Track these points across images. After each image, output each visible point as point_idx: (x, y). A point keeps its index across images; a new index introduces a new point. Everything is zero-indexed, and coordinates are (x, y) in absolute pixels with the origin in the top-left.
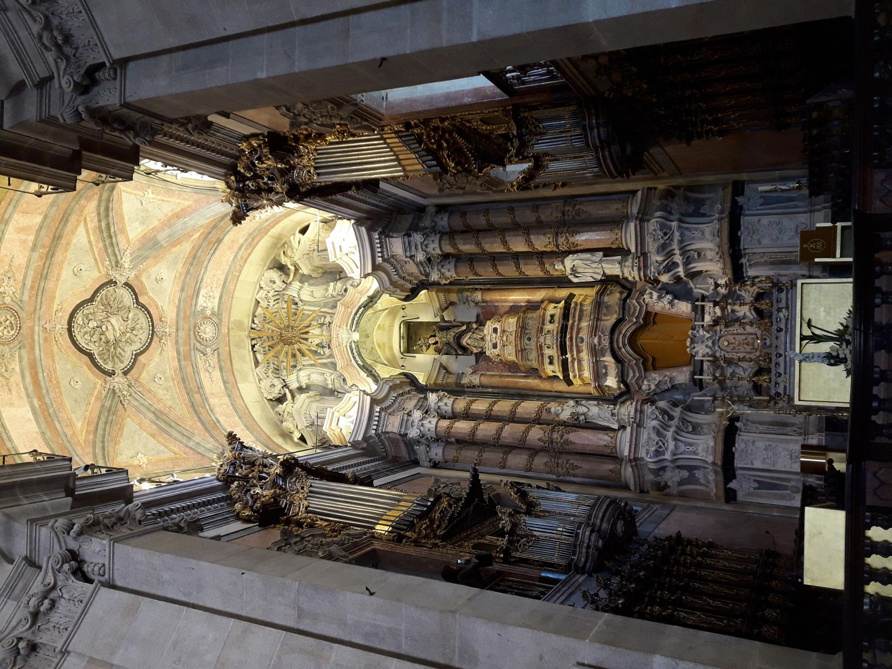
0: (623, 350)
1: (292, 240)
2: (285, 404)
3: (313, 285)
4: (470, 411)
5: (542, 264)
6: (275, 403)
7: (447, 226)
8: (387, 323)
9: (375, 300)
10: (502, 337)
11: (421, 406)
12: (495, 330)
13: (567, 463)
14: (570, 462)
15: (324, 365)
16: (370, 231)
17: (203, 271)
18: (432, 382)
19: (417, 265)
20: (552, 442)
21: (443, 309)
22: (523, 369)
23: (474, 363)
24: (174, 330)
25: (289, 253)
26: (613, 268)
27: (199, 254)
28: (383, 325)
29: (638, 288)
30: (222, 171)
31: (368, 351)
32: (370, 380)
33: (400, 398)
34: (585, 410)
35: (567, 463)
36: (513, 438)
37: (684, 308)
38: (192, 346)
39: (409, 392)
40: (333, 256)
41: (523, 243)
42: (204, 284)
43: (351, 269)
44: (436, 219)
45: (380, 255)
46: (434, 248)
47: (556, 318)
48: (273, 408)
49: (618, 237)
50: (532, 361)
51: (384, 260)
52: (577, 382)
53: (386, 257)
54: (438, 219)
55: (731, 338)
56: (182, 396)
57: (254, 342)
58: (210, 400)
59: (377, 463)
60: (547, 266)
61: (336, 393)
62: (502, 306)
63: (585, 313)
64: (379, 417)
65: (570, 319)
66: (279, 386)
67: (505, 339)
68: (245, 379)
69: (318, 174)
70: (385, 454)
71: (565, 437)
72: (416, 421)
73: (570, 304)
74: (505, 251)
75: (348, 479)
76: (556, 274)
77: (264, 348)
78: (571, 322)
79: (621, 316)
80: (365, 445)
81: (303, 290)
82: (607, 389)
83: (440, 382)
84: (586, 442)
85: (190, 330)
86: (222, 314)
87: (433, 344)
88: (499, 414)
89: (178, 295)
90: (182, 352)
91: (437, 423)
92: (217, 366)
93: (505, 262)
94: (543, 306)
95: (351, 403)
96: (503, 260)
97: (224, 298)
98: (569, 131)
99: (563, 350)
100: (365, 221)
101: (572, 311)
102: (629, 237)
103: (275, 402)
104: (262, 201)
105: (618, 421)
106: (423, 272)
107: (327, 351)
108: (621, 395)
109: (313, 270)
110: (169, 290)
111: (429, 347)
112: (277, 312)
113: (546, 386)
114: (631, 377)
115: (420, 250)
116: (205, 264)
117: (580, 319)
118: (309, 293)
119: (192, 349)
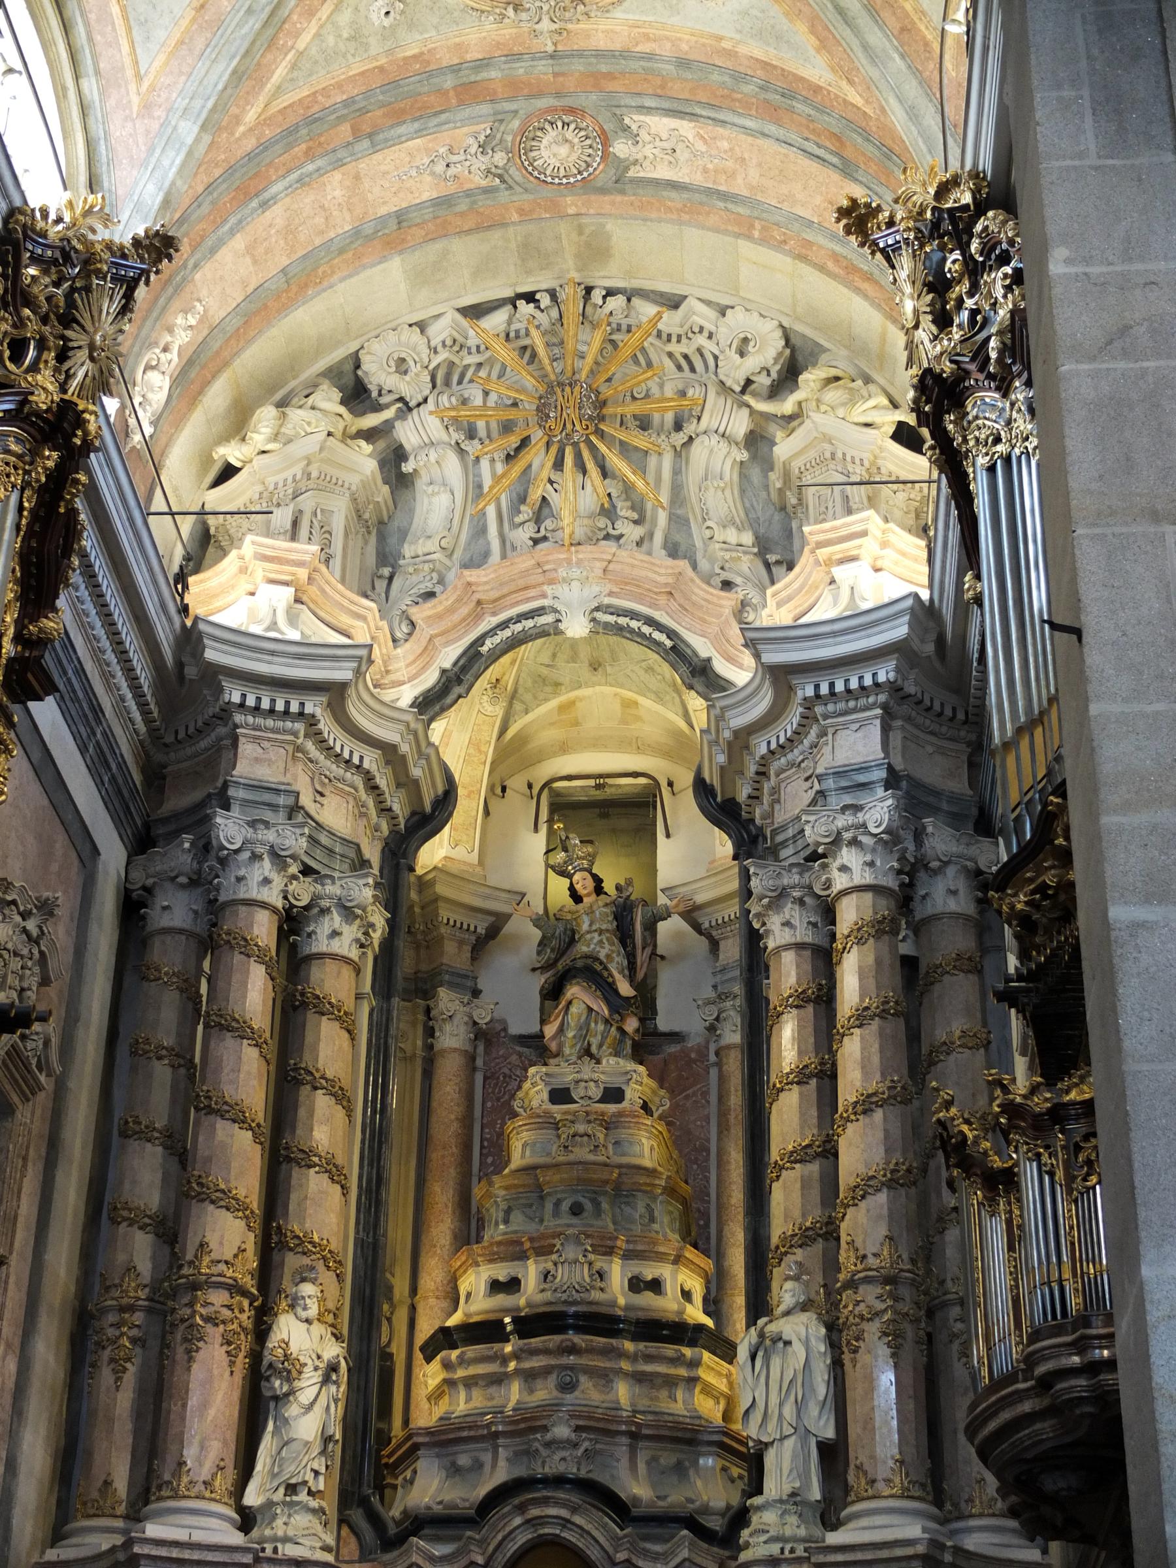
0: (518, 1521)
1: (872, 403)
2: (342, 410)
3: (743, 476)
4: (311, 1016)
5: (805, 1237)
6: (349, 380)
7: (929, 909)
8: (651, 731)
9: (698, 683)
10: (588, 1118)
11: (331, 851)
12: (614, 1095)
13: (134, 1341)
14: (138, 1350)
17: (749, 123)
18: (440, 889)
19: (798, 818)
20: (195, 1287)
21: (691, 914)
23: (514, 1030)
24: (550, 48)
25: (833, 395)
27: (799, 106)
28: (639, 718)
30: (986, 163)
31: (545, 671)
32: (430, 678)
33: (358, 781)
34: (306, 1397)
35: (134, 1341)
36: (209, 1160)
38: (508, 106)
39: (385, 810)
40: (821, 537)
41: (862, 1170)
42: (709, 130)
43: (789, 599)
44: (951, 871)
45: (824, 689)
47: (647, 1299)
48: (333, 374)
49: (880, 1486)
50: (506, 1221)
51: (809, 704)
53: (819, 710)
54: (952, 878)
56: (339, 86)
57: (545, 300)
58: (337, 176)
59: (137, 715)
61: (386, 571)
62: (707, 1119)
63: (664, 1393)
64: (286, 712)
65: (641, 1345)
67: (581, 1128)
68: (419, 278)
69: (991, 469)
70: (169, 739)
71: (209, 1328)
72: (270, 836)
73: (692, 1343)
74: (840, 1109)
75: (34, 619)
76: (775, 1285)
77: (527, 334)
78: (629, 1346)
79: (635, 1511)
80: (191, 672)
81: (724, 445)
82: (408, 1474)
83: (445, 914)
84: (193, 1401)
85: (558, 95)
86: (622, 192)
87: (572, 889)
88: (302, 1113)
89: (666, 50)
90: (484, 75)
91: (264, 905)
92: (451, 188)
93: (814, 1112)
94: (690, 1253)
95: (345, 620)
96: (819, 1108)
97: (674, 194)
98: (1075, 1275)
99: (529, 1325)
100: (934, 636)
101: (669, 1350)
103: (352, 377)
104: (912, 298)
105: (270, 1504)
106: (780, 838)
107: (523, 535)
108: (375, 1520)
109: (786, 475)
110: (675, 20)
111: (563, 873)
112: (649, 365)
113: (432, 1277)
115: (842, 821)
116: (772, 129)
117: (639, 1378)
119: (498, 107)
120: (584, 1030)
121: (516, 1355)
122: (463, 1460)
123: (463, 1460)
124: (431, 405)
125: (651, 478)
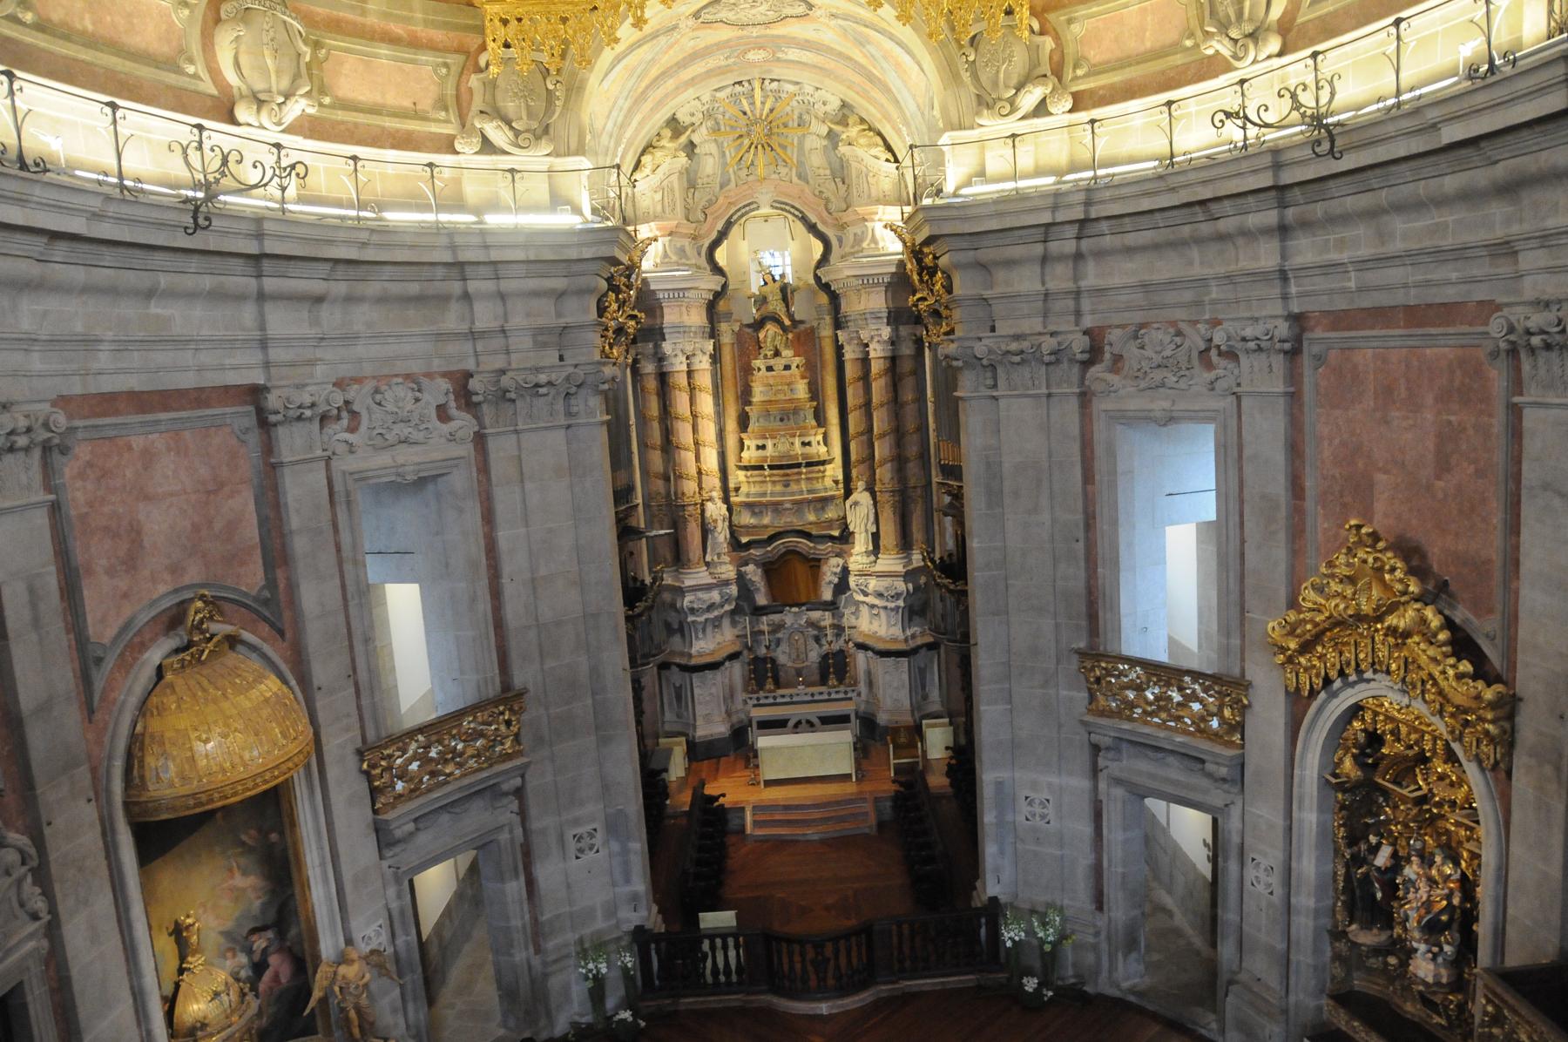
4: (698, 393)
12: (787, 367)
15: (724, 173)
16: (893, 274)
22: (747, 408)
25: (862, 141)
26: (861, 544)
29: (844, 547)
34: (719, 529)
37: (827, 595)
46: (877, 351)
52: (741, 475)
55: (802, 641)
57: (746, 84)
60: (862, 467)
66: (693, 119)
101: (816, 468)
102: (890, 562)
114: (755, 552)
117: (808, 479)
118: (814, 146)
120: (774, 339)
121: (770, 476)
122: (757, 510)
123: (757, 510)
124: (703, 130)
125: (789, 152)
